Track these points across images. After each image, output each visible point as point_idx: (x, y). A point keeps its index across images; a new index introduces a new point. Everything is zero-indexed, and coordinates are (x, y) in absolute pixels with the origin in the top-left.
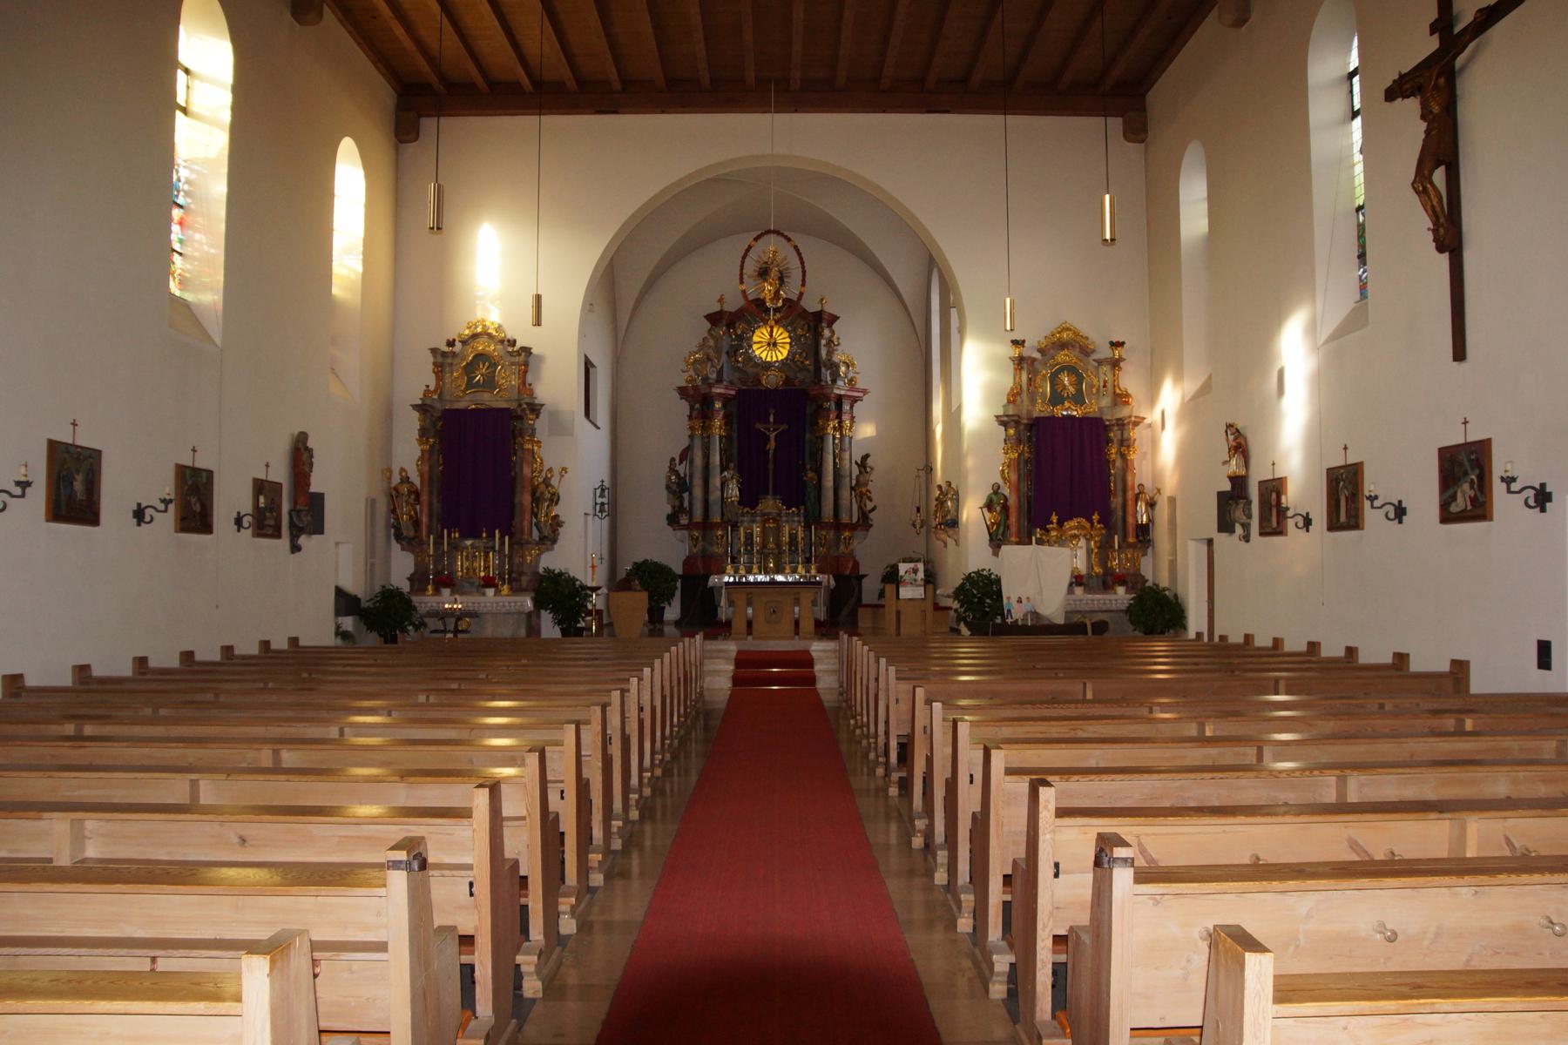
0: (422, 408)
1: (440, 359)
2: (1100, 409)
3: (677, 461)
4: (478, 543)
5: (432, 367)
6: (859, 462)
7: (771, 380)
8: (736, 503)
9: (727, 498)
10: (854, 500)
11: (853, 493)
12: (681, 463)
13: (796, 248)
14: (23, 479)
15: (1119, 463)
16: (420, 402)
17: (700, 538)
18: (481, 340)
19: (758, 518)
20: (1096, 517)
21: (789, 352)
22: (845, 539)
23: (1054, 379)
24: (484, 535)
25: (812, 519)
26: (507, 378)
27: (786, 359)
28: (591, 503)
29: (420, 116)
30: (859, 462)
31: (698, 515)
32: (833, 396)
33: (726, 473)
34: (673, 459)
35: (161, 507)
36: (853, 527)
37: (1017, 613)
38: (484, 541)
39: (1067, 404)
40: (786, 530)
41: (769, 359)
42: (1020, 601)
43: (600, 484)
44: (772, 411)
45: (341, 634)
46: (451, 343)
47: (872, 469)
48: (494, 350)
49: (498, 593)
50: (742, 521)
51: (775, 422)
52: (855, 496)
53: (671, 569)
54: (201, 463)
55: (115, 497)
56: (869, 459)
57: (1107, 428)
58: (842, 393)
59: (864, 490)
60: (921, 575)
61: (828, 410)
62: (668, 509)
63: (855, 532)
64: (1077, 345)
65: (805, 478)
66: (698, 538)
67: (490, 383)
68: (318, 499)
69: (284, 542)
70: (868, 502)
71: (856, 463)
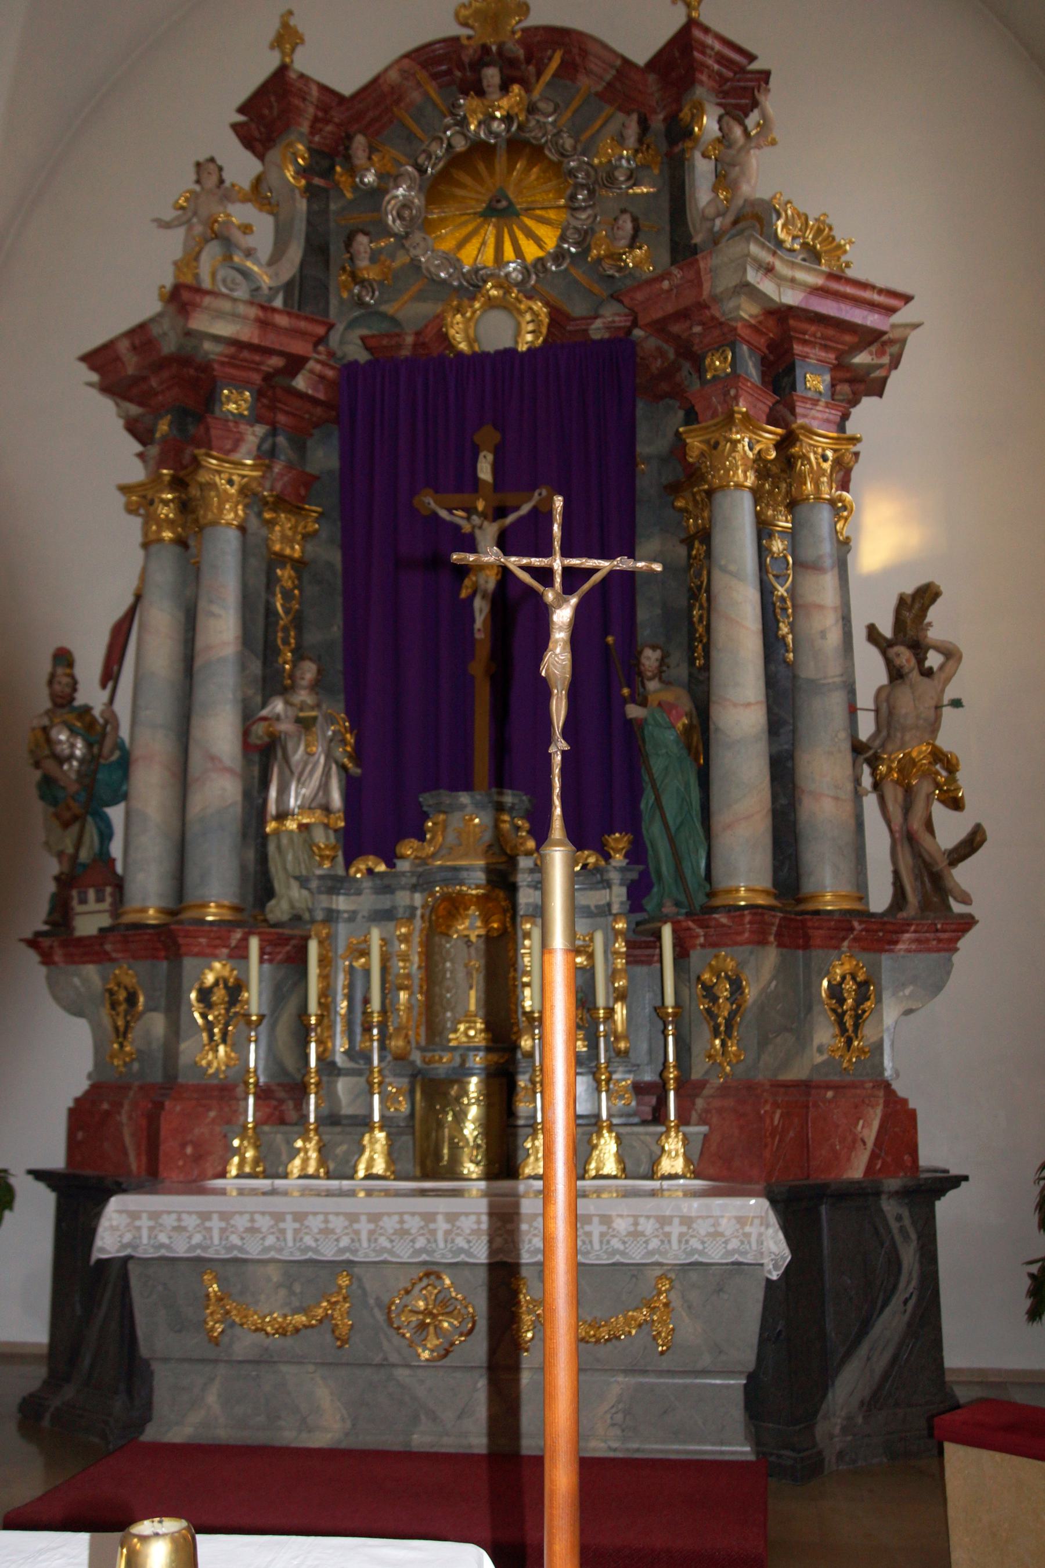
6: (887, 630)
8: (320, 838)
9: (282, 816)
10: (870, 802)
11: (866, 770)
22: (836, 992)
30: (887, 630)
32: (748, 310)
44: (488, 435)
47: (951, 654)
50: (331, 916)
52: (876, 786)
56: (934, 614)
58: (791, 298)
59: (920, 751)
63: (886, 960)
65: (633, 711)
70: (939, 812)
71: (873, 634)
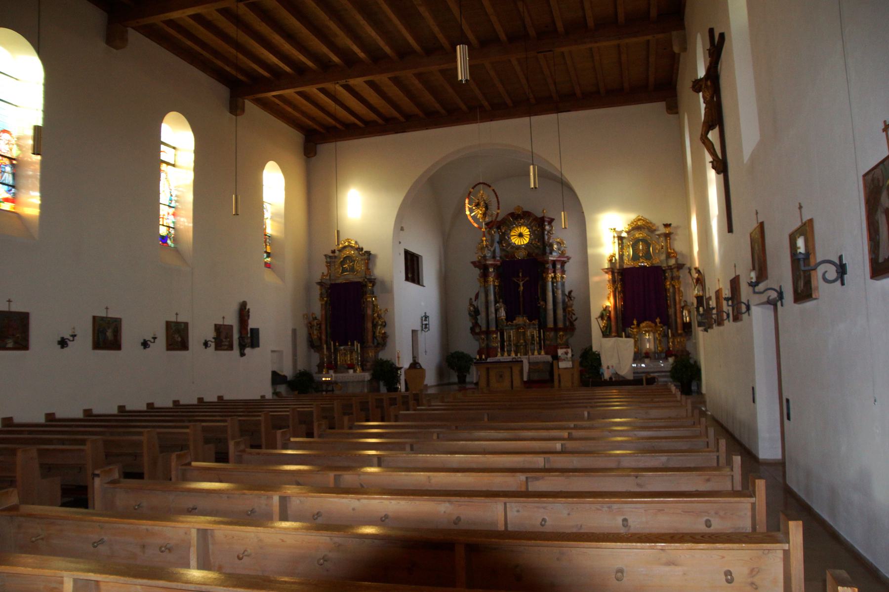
0: (320, 284)
1: (329, 260)
2: (661, 261)
3: (473, 300)
4: (348, 347)
5: (325, 263)
7: (520, 255)
8: (504, 320)
12: (475, 300)
13: (493, 190)
14: (73, 334)
15: (671, 290)
16: (320, 281)
17: (485, 339)
18: (347, 249)
19: (514, 327)
20: (658, 320)
21: (529, 239)
23: (635, 246)
24: (349, 344)
25: (542, 326)
26: (360, 267)
27: (528, 243)
28: (420, 324)
29: (316, 144)
31: (484, 328)
33: (498, 305)
34: (471, 299)
35: (152, 340)
36: (565, 329)
37: (607, 376)
38: (350, 346)
39: (641, 260)
40: (529, 333)
41: (519, 244)
42: (608, 368)
43: (424, 314)
45: (275, 393)
46: (333, 252)
47: (574, 298)
48: (354, 254)
49: (355, 371)
51: (522, 277)
53: (469, 356)
54: (181, 319)
55: (129, 336)
57: (664, 271)
58: (555, 259)
60: (570, 355)
61: (548, 269)
62: (470, 325)
64: (646, 228)
65: (539, 305)
66: (484, 339)
67: (352, 269)
68: (255, 332)
69: (236, 351)
